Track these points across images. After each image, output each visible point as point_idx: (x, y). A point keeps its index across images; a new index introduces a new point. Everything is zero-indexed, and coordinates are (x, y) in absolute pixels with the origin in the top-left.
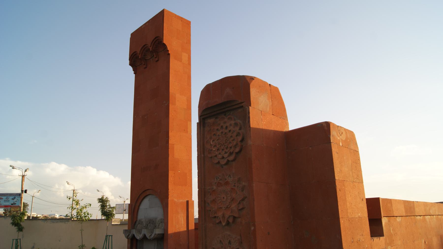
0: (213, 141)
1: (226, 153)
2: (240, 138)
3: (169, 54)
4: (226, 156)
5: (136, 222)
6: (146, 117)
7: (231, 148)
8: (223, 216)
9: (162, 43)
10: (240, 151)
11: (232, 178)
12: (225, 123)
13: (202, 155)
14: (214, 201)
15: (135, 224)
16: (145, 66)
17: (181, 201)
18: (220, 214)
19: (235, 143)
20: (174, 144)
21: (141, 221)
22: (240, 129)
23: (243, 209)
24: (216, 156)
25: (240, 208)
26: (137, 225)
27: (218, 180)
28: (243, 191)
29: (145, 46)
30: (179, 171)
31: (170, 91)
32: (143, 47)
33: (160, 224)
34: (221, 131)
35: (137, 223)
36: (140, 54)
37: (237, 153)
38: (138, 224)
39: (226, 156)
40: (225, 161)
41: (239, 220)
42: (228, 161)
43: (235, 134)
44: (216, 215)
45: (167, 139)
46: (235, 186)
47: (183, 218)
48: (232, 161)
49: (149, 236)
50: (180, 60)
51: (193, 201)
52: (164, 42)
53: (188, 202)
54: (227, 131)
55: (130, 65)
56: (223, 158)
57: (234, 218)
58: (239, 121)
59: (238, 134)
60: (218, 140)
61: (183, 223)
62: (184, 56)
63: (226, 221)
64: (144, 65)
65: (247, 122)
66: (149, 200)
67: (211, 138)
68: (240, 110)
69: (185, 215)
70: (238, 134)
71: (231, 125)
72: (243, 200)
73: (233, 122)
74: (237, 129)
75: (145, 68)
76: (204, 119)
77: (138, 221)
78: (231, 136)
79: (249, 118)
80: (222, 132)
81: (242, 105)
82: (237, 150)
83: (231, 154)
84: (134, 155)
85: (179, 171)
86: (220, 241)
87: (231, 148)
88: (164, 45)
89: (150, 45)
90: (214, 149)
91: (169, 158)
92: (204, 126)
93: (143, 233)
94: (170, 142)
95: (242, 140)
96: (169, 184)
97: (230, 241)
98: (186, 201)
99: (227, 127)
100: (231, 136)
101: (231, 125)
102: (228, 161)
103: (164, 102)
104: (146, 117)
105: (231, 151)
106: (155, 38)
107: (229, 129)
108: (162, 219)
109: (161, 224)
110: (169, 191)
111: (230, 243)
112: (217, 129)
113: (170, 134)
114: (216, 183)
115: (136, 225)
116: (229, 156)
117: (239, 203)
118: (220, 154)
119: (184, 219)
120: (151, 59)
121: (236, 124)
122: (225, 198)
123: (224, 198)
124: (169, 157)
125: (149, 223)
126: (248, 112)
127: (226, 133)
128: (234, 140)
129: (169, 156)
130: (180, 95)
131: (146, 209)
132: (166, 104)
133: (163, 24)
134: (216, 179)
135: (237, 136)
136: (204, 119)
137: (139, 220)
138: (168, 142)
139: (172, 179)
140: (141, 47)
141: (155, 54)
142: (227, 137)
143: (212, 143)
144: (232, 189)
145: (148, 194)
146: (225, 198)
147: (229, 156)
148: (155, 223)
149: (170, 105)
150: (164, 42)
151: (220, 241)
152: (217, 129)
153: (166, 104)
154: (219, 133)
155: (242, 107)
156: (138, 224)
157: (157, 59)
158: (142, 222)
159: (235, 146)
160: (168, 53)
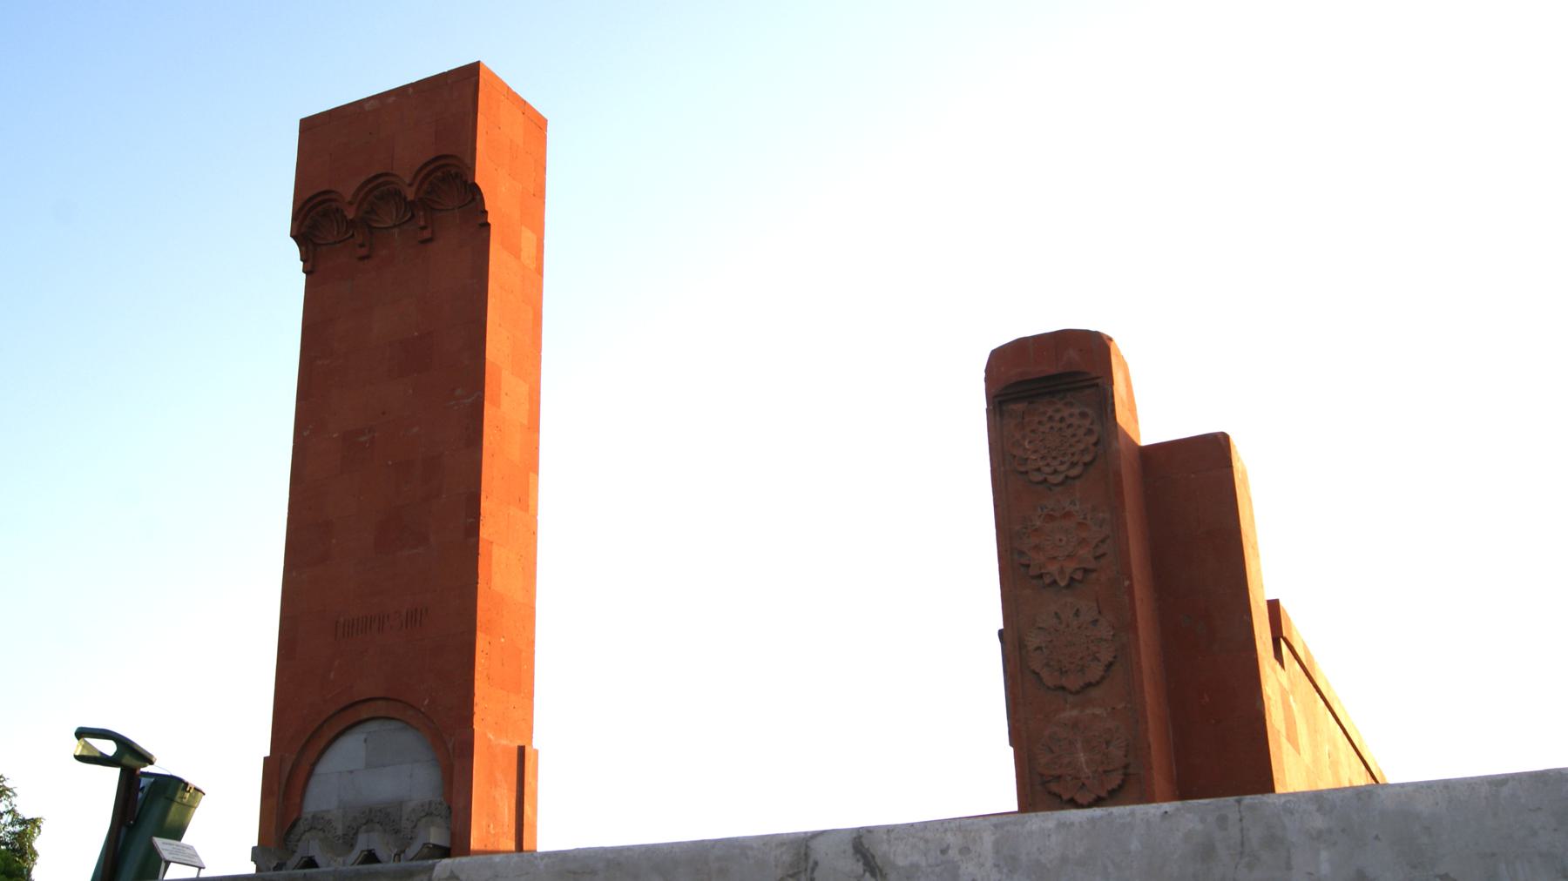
0: (1030, 442)
1: (1062, 463)
2: (1093, 439)
3: (488, 225)
4: (1047, 470)
5: (294, 825)
6: (363, 439)
7: (1073, 454)
8: (1062, 571)
9: (470, 182)
10: (1091, 463)
11: (1078, 506)
12: (1058, 411)
13: (1002, 469)
14: (1037, 548)
15: (289, 832)
16: (364, 252)
17: (504, 742)
18: (1053, 568)
19: (1082, 446)
20: (492, 543)
21: (323, 818)
22: (1092, 424)
23: (1103, 555)
24: (1039, 470)
25: (1097, 554)
26: (301, 837)
27: (1045, 510)
28: (1101, 526)
29: (381, 180)
30: (504, 637)
31: (487, 356)
32: (369, 181)
33: (419, 820)
34: (1049, 425)
35: (302, 826)
36: (351, 203)
37: (1085, 464)
38: (305, 831)
39: (1063, 468)
40: (1060, 478)
41: (1094, 575)
42: (1067, 477)
43: (1081, 432)
44: (1043, 571)
45: (472, 520)
46: (1085, 518)
47: (507, 804)
48: (1074, 478)
49: (393, 855)
50: (516, 252)
51: (536, 752)
52: (476, 181)
53: (521, 751)
54: (1063, 425)
55: (294, 236)
56: (1055, 472)
57: (1086, 571)
58: (1089, 411)
59: (1090, 432)
60: (1041, 441)
61: (506, 820)
62: (527, 236)
63: (1067, 578)
64: (362, 246)
65: (1109, 411)
66: (365, 741)
67: (1024, 438)
68: (1088, 391)
69: (514, 794)
70: (1090, 432)
71: (1071, 415)
72: (1103, 541)
73: (1076, 411)
74: (1087, 423)
75: (362, 258)
76: (1001, 403)
77: (306, 820)
78: (1074, 435)
79: (1113, 404)
80: (1052, 428)
81: (1098, 381)
82: (1087, 458)
83: (1073, 465)
84: (294, 574)
85: (503, 640)
86: (1056, 613)
87: (1073, 454)
88: (476, 189)
89: (407, 180)
90: (1033, 457)
91: (476, 588)
92: (1002, 415)
93: (365, 848)
94: (485, 532)
95: (1096, 444)
96: (477, 676)
97: (1078, 610)
98: (516, 745)
99: (1062, 420)
100: (1074, 435)
101: (1071, 415)
102: (1067, 477)
103: (459, 392)
104: (363, 439)
105: (1075, 459)
106: (438, 158)
107: (1069, 422)
108: (430, 803)
109: (424, 820)
110: (476, 700)
111: (1077, 614)
112: (1040, 423)
113: (485, 504)
114: (1040, 516)
115: (292, 836)
116: (1068, 470)
117: (1097, 546)
118: (1048, 465)
119: (509, 807)
120: (396, 231)
121: (1083, 415)
122: (1065, 539)
123: (1061, 540)
124: (477, 583)
125: (364, 821)
126: (1110, 394)
127: (1060, 429)
128: (1079, 441)
129: (479, 581)
130: (512, 374)
131: (351, 772)
132: (470, 400)
133: (477, 114)
134: (1039, 510)
135: (1085, 435)
136: (1001, 403)
137: (314, 817)
138: (473, 529)
139: (483, 661)
140: (363, 179)
141: (421, 213)
142: (1065, 436)
143: (1027, 447)
144: (1079, 523)
145: (365, 716)
146: (1065, 539)
147: (1068, 470)
148: (394, 821)
149: (485, 403)
150: (478, 181)
151: (1056, 613)
152: (1040, 423)
153: (470, 400)
154: (1042, 429)
155: (1097, 385)
156: (305, 831)
157: (427, 234)
158: (329, 822)
159: (1083, 452)
160: (481, 221)
